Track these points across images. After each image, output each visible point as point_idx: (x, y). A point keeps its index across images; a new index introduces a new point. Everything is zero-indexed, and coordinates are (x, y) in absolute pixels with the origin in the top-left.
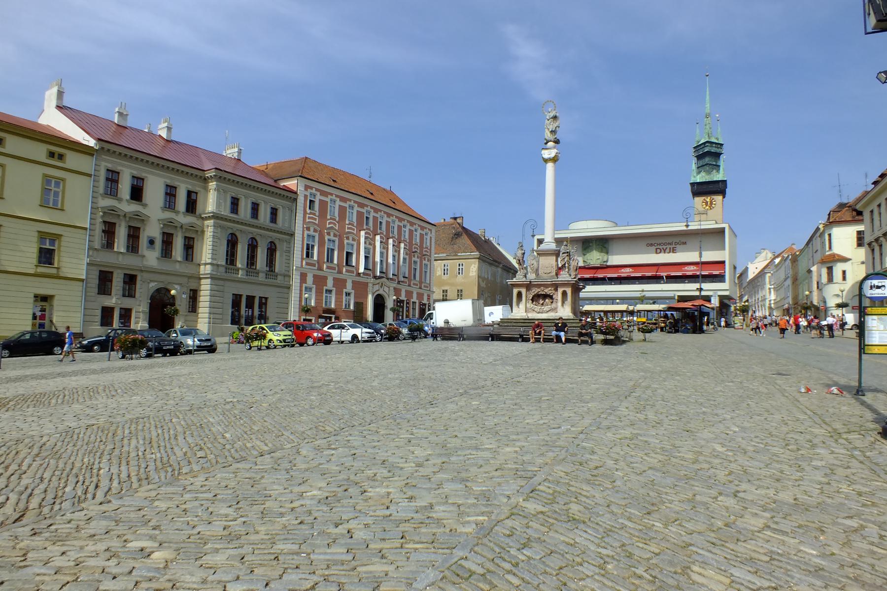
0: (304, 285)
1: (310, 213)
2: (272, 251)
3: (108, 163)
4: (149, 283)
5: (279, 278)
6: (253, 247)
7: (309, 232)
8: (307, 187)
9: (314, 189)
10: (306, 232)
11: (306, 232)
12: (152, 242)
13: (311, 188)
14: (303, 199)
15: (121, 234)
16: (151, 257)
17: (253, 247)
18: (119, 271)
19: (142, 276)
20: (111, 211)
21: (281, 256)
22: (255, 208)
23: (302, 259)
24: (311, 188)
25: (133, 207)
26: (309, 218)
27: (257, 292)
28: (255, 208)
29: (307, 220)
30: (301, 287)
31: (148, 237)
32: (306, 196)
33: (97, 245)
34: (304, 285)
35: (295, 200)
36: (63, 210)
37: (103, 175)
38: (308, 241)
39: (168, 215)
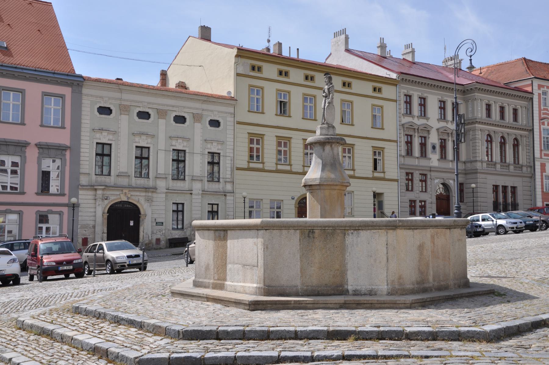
0: (544, 174)
1: (544, 109)
2: (516, 146)
3: (405, 89)
4: (434, 180)
5: (524, 169)
6: (503, 144)
7: (544, 126)
8: (540, 86)
9: (545, 87)
10: (542, 126)
11: (542, 126)
12: (434, 147)
13: (543, 86)
14: (537, 97)
15: (416, 142)
16: (434, 159)
17: (503, 144)
18: (417, 172)
19: (431, 175)
20: (411, 127)
21: (523, 150)
22: (502, 109)
23: (541, 150)
24: (543, 86)
25: (422, 121)
26: (544, 114)
27: (509, 182)
28: (502, 109)
29: (542, 116)
30: (542, 176)
31: (432, 144)
32: (539, 94)
33: (403, 153)
34: (544, 174)
35: (532, 99)
36: (384, 129)
37: (403, 99)
38: (544, 134)
39: (443, 124)
